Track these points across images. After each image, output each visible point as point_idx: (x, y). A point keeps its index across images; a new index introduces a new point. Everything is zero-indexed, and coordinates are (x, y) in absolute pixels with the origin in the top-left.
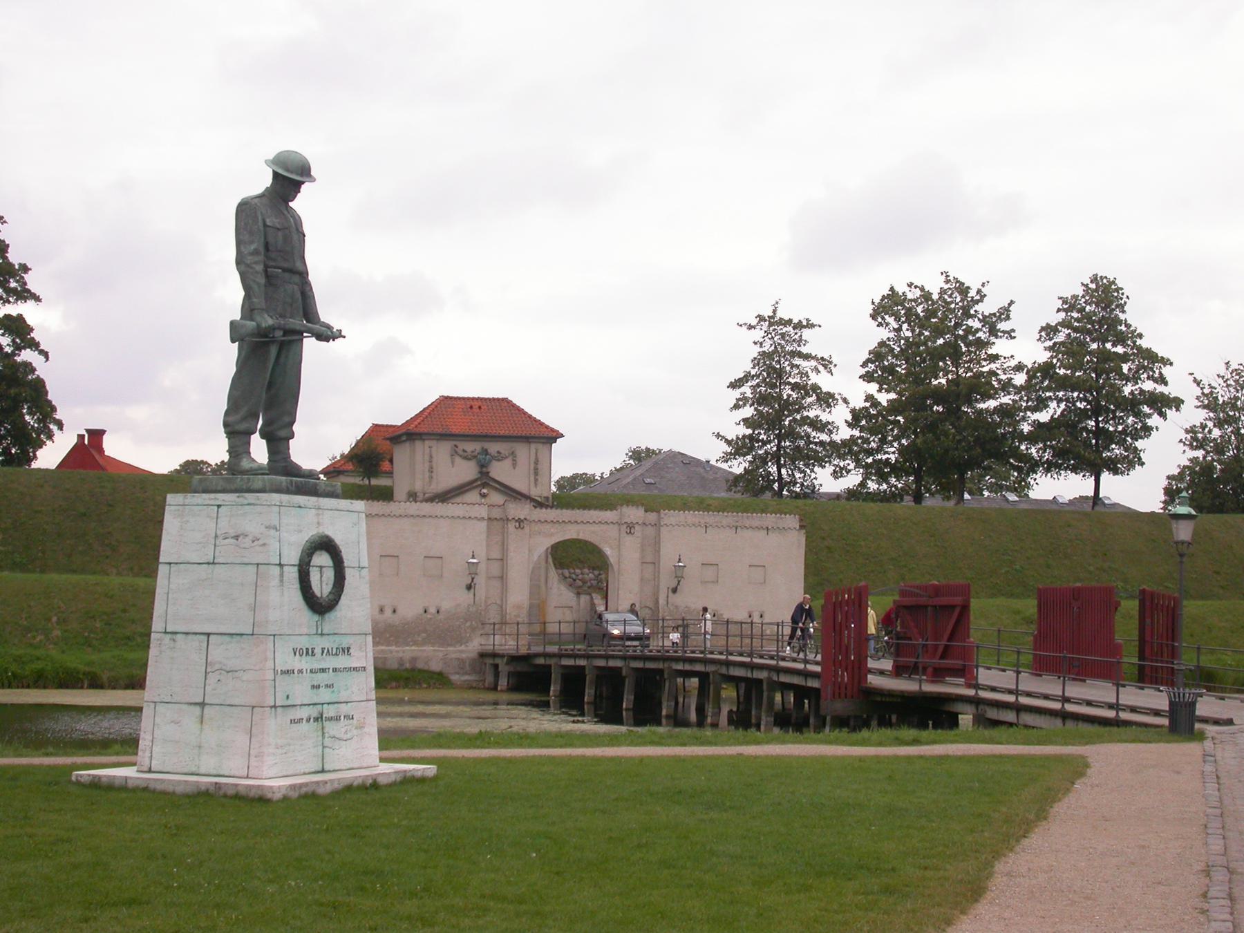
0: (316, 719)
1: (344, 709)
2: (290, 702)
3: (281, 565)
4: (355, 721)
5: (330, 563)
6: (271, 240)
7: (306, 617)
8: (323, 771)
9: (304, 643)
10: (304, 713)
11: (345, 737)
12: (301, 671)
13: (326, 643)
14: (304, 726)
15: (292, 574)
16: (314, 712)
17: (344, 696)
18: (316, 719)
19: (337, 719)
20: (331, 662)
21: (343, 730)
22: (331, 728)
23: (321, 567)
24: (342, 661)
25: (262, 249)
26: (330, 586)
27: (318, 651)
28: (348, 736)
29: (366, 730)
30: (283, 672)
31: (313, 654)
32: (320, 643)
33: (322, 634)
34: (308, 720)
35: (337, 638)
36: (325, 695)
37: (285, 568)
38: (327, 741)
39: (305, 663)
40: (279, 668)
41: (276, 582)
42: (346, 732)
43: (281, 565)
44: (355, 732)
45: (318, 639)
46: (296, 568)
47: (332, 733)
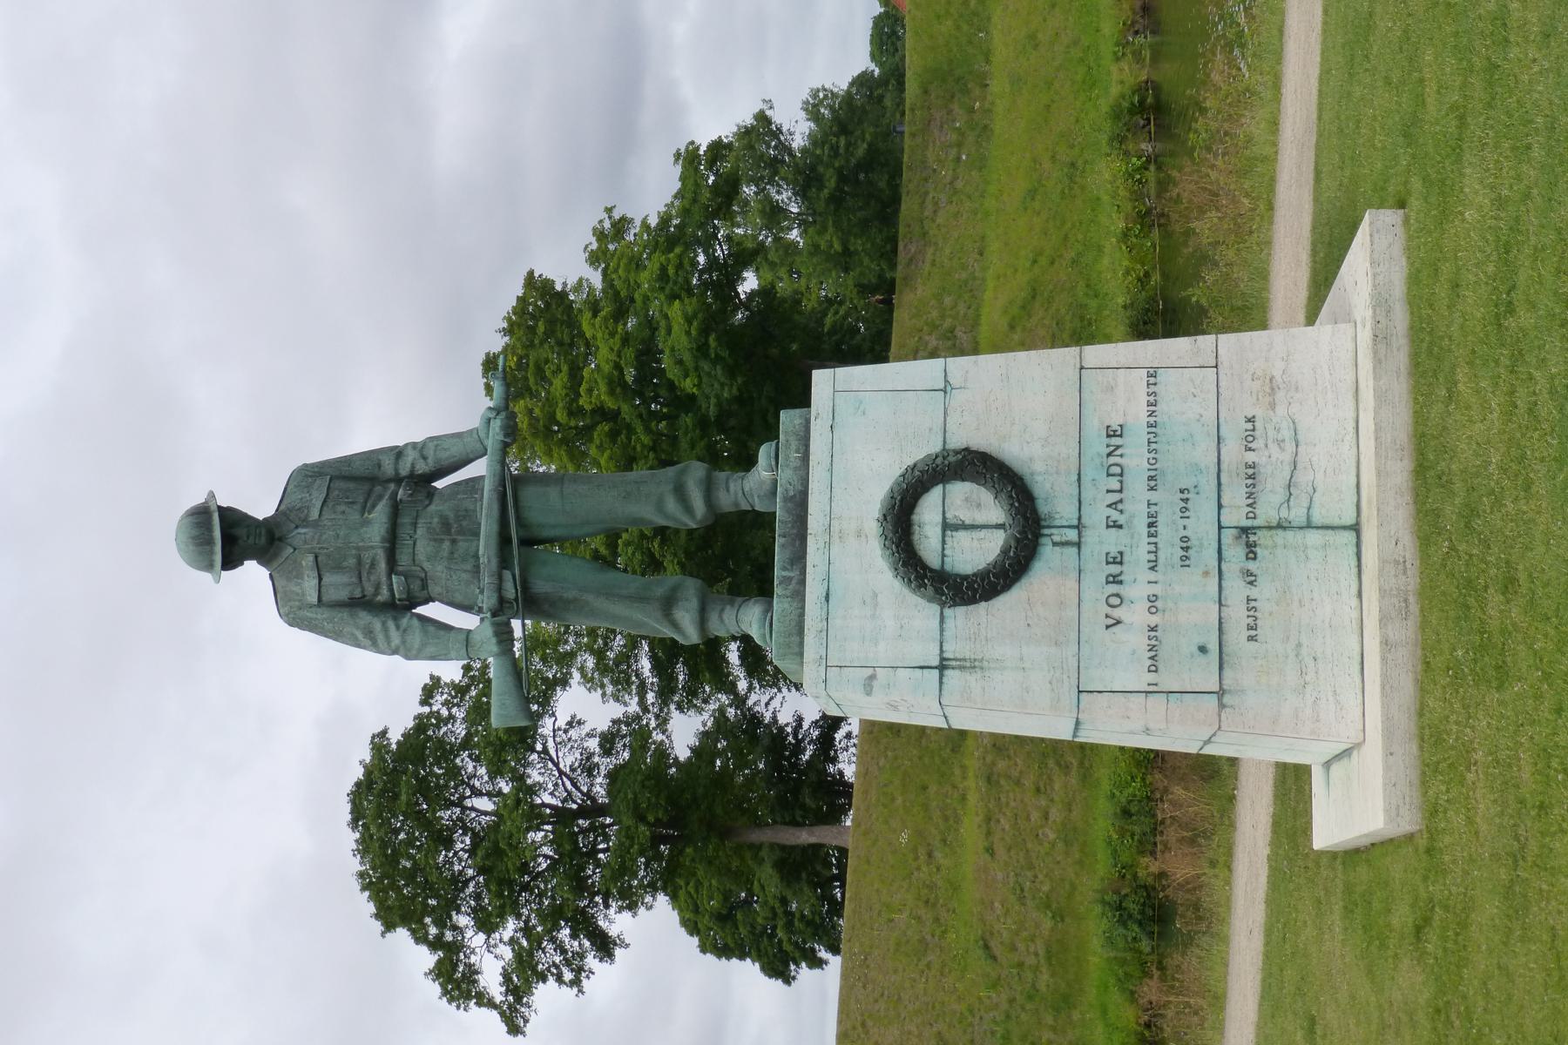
0: (1251, 552)
1: (1233, 452)
2: (1213, 647)
3: (942, 667)
4: (1258, 412)
5: (937, 491)
6: (343, 595)
8: (1356, 528)
9: (1095, 589)
11: (1290, 447)
13: (1097, 514)
14: (1265, 591)
15: (959, 617)
16: (1234, 553)
17: (1204, 453)
18: (1251, 552)
19: (1252, 475)
23: (947, 526)
24: (1135, 458)
25: (364, 617)
26: (984, 495)
27: (1113, 541)
28: (1287, 434)
29: (1277, 373)
30: (1153, 669)
31: (1118, 560)
32: (1100, 541)
33: (1079, 527)
34: (1250, 578)
35: (1085, 479)
36: (1202, 525)
38: (1297, 514)
39: (1137, 588)
40: (1141, 680)
41: (972, 679)
42: (1280, 443)
43: (942, 667)
44: (1281, 410)
45: (1090, 537)
46: (948, 612)
47: (1280, 496)
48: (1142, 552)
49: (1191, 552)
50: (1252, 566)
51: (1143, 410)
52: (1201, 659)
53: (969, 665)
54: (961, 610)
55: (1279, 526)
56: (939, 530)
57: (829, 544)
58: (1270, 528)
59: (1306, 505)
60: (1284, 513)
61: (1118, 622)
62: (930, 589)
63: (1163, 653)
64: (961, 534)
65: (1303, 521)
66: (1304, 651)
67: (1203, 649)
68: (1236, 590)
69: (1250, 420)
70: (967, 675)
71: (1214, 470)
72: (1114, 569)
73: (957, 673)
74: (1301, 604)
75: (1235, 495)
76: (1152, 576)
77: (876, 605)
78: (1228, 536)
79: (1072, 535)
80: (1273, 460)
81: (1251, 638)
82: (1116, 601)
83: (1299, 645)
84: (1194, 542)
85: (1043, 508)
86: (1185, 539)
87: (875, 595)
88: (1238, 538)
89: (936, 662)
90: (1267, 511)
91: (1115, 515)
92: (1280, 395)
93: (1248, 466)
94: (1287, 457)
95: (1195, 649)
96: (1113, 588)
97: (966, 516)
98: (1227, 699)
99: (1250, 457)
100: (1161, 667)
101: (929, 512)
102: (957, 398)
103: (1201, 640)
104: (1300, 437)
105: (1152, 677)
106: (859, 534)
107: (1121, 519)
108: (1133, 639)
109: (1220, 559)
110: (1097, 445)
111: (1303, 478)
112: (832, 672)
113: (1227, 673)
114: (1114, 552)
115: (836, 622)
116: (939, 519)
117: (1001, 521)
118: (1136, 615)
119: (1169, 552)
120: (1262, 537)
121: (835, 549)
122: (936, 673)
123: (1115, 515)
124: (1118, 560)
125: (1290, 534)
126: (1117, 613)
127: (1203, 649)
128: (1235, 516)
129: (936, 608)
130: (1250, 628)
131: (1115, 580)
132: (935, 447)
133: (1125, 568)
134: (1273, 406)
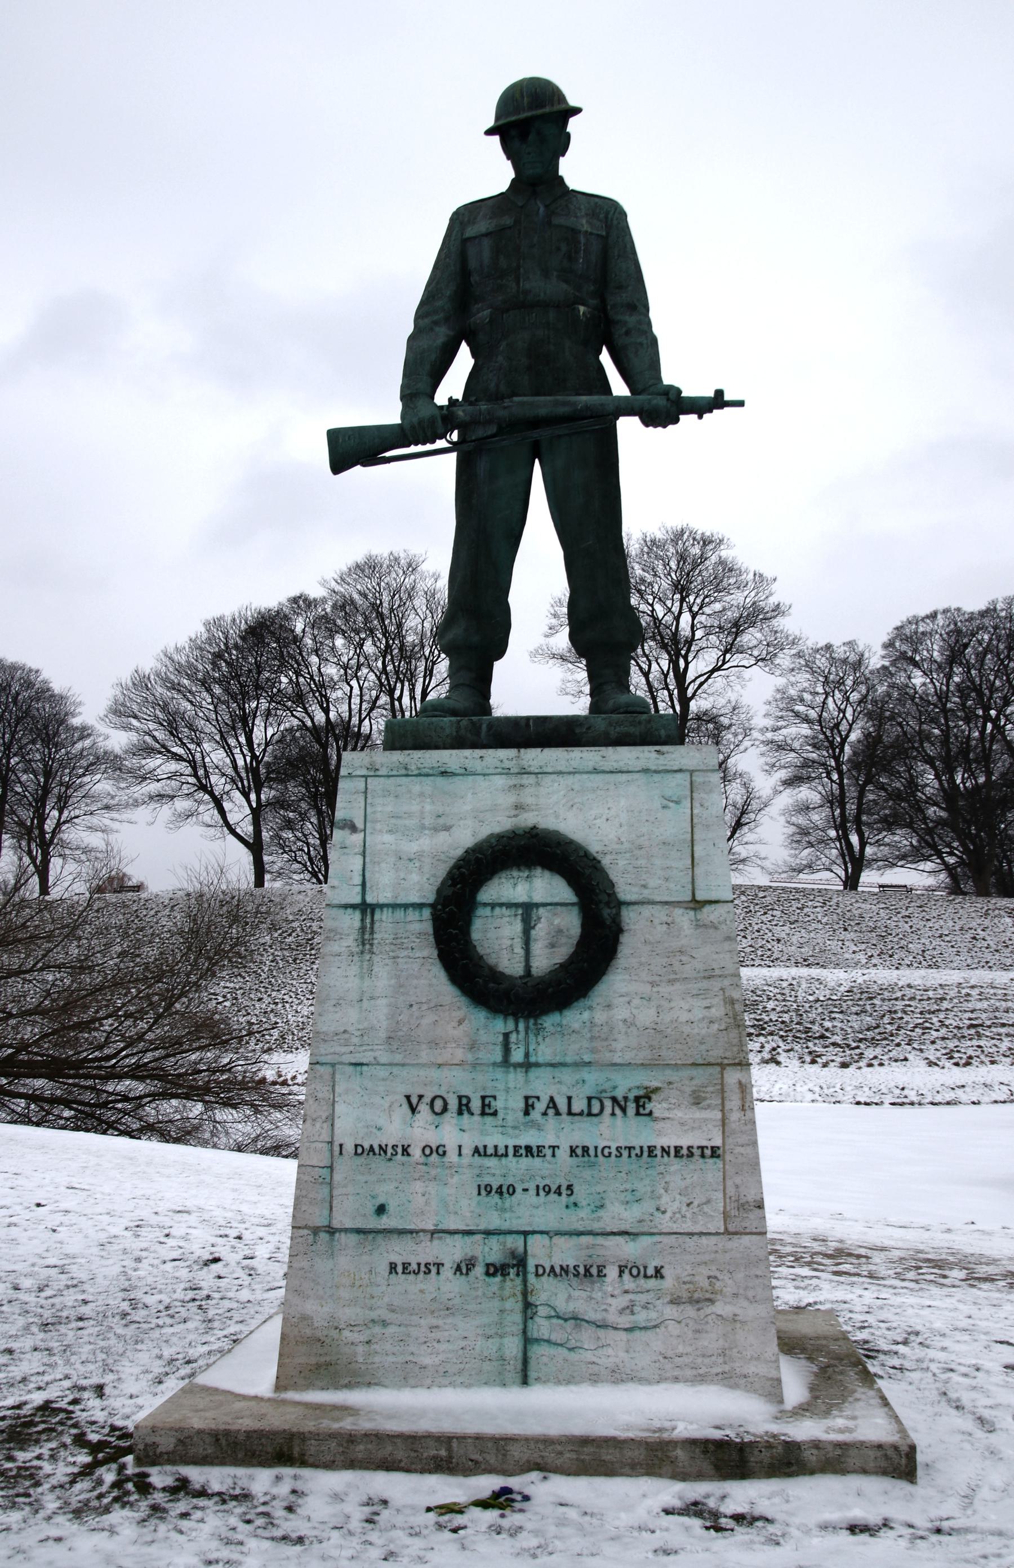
0: (494, 1270)
2: (385, 1222)
3: (366, 909)
7: (463, 1029)
9: (456, 1082)
10: (452, 1251)
11: (625, 1321)
12: (441, 1151)
13: (543, 1085)
14: (449, 1285)
15: (421, 924)
16: (493, 1251)
17: (619, 1214)
18: (494, 1270)
19: (589, 1273)
20: (552, 1133)
21: (623, 1301)
22: (550, 1293)
24: (614, 1131)
26: (563, 953)
27: (510, 1104)
28: (641, 1317)
29: (720, 1308)
30: (359, 1151)
31: (487, 1110)
33: (527, 1065)
34: (464, 1267)
35: (585, 1074)
37: (384, 918)
38: (541, 1327)
39: (451, 1133)
41: (350, 942)
42: (630, 1309)
43: (366, 909)
45: (515, 1078)
46: (427, 913)
47: (562, 1305)
48: (494, 1139)
49: (495, 1198)
50: (479, 1270)
51: (670, 1141)
52: (371, 1208)
53: (366, 937)
54: (428, 927)
55: (527, 1305)
56: (523, 898)
57: (507, 772)
58: (525, 1293)
59: (554, 1337)
60: (542, 1311)
61: (413, 1110)
62: (449, 892)
63: (378, 1163)
64: (518, 927)
65: (533, 1333)
66: (377, 1330)
67: (381, 1210)
68: (452, 1251)
69: (658, 1273)
70: (355, 935)
71: (596, 1226)
72: (476, 1105)
73: (357, 924)
74: (433, 1328)
75: (567, 1253)
76: (467, 1151)
77: (436, 829)
78: (516, 1243)
79: (517, 1056)
80: (611, 1296)
81: (393, 1267)
82: (438, 1105)
83: (385, 1324)
84: (509, 1201)
85: (549, 1021)
86: (512, 1190)
87: (447, 828)
88: (513, 1254)
89: (369, 899)
90: (550, 1293)
91: (540, 1106)
92: (690, 1311)
93: (600, 1269)
94: (612, 1318)
95: (381, 1200)
96: (453, 1104)
97: (541, 931)
98: (324, 1236)
99: (612, 1272)
100: (361, 1160)
101: (544, 887)
102: (684, 918)
103: (391, 1208)
104: (637, 1334)
105: (349, 1148)
106: (519, 807)
107: (536, 1115)
108: (394, 1127)
109: (488, 1233)
110: (625, 1084)
111: (586, 1336)
112: (361, 784)
113: (354, 1238)
114: (498, 1104)
115: (417, 786)
116: (537, 898)
117: (534, 971)
118: (422, 1130)
119: (496, 1171)
120: (513, 1283)
121: (500, 781)
122: (357, 900)
123: (540, 1106)
124: (487, 1110)
125: (518, 1318)
126: (424, 1108)
127: (381, 1210)
128: (539, 1251)
129: (431, 898)
130: (406, 1266)
131: (464, 1106)
132: (625, 891)
133: (477, 1118)
134: (675, 1301)
